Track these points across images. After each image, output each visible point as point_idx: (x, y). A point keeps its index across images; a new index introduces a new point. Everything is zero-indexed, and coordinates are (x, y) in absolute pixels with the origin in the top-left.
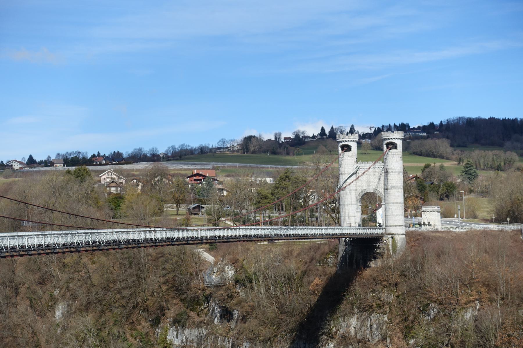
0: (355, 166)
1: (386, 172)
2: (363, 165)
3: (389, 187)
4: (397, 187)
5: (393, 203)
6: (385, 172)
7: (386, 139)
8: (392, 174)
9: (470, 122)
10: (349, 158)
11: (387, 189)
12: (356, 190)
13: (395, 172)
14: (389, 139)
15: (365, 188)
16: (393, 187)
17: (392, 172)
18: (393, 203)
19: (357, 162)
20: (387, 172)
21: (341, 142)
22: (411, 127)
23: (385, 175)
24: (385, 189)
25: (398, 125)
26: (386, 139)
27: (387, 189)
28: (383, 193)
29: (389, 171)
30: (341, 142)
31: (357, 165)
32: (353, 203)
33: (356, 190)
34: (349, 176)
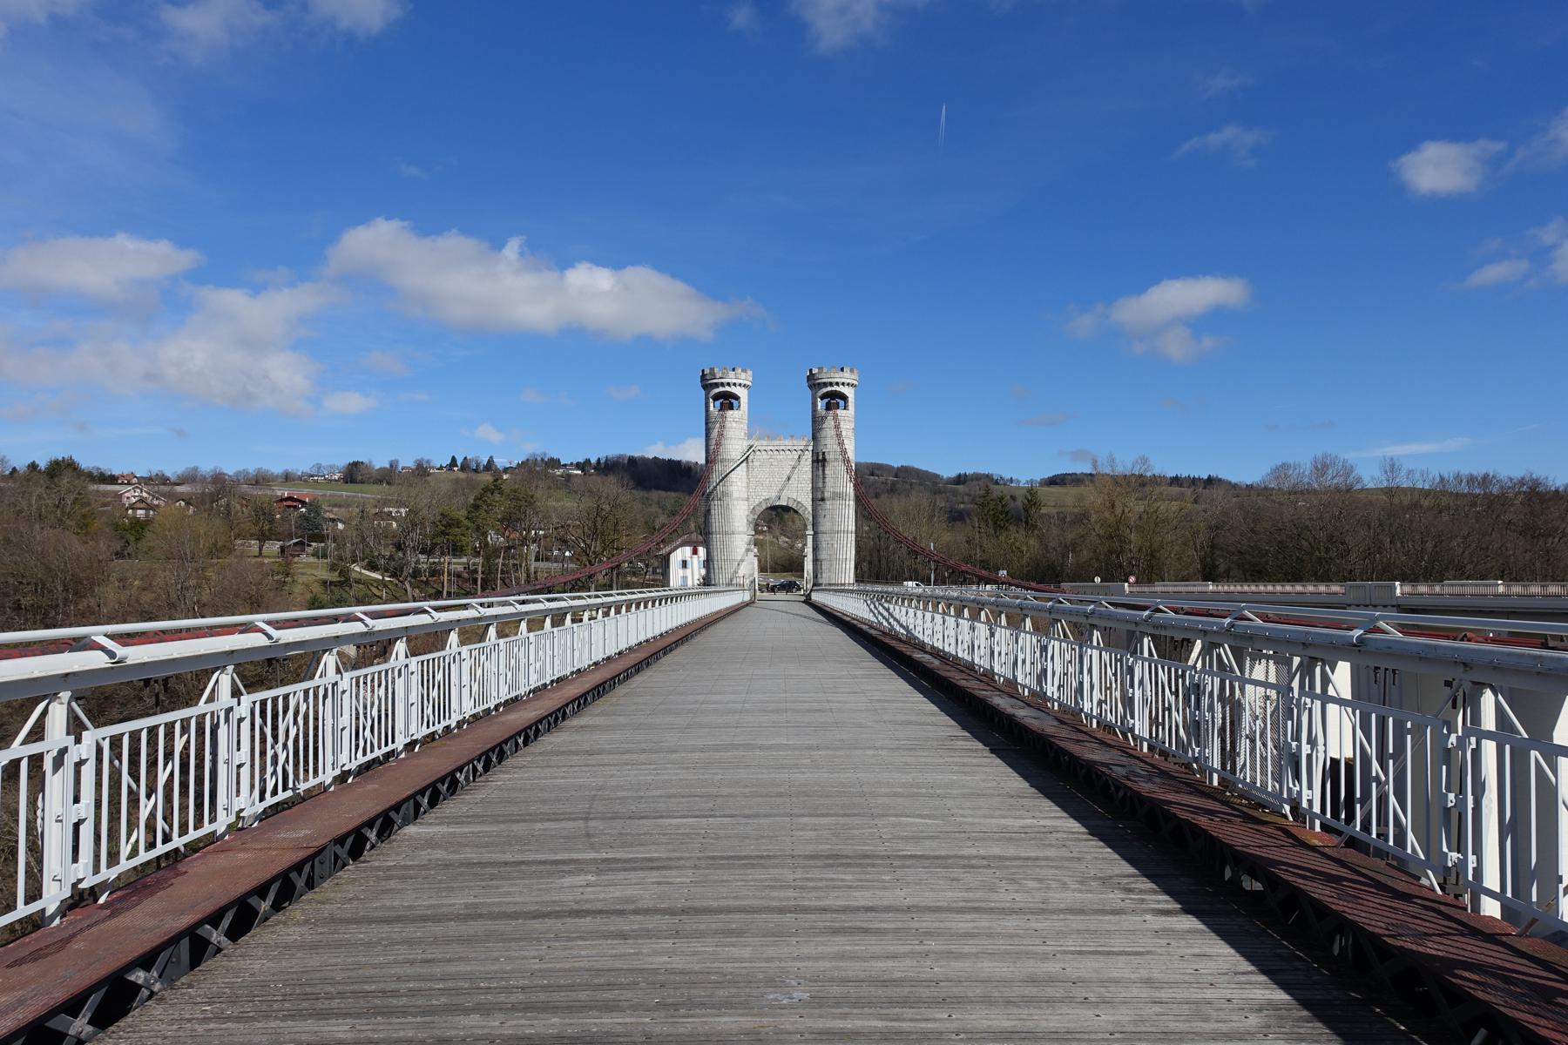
0: (746, 444)
7: (825, 385)
11: (823, 499)
14: (831, 384)
15: (765, 495)
16: (838, 496)
20: (824, 460)
21: (716, 385)
26: (825, 385)
27: (823, 499)
30: (716, 385)
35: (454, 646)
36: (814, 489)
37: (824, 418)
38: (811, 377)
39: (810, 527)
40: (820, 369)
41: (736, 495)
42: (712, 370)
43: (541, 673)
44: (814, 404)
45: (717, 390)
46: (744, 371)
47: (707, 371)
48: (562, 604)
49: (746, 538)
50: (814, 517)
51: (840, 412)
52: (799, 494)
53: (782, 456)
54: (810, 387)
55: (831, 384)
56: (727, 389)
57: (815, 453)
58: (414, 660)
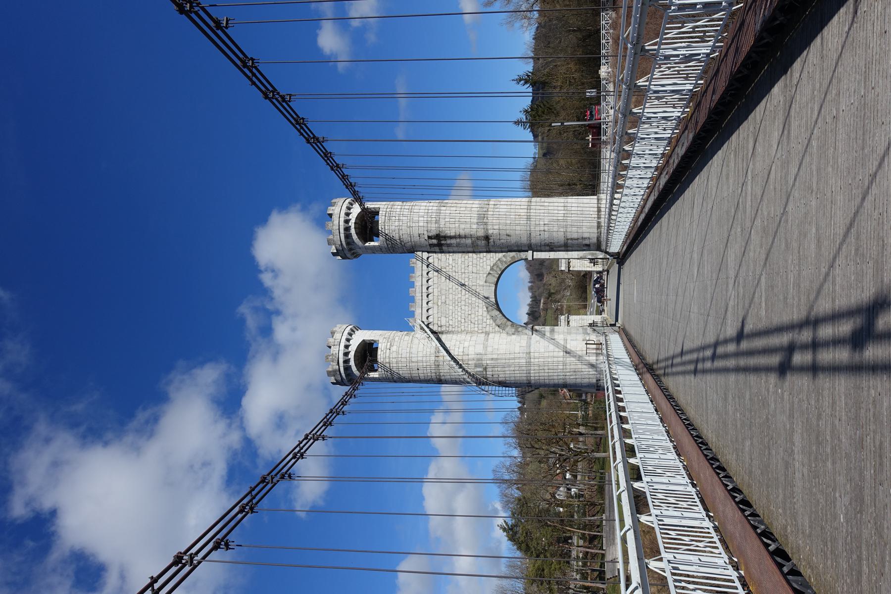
0: (419, 334)
1: (440, 243)
3: (481, 233)
5: (529, 218)
7: (348, 236)
8: (442, 222)
10: (394, 348)
11: (487, 238)
13: (439, 213)
14: (347, 229)
16: (482, 218)
17: (437, 222)
18: (529, 218)
19: (411, 329)
20: (438, 237)
24: (489, 252)
26: (348, 236)
28: (500, 255)
29: (433, 229)
31: (417, 328)
32: (524, 343)
33: (487, 333)
34: (441, 348)
35: (649, 518)
37: (388, 239)
41: (480, 349)
42: (329, 374)
43: (675, 470)
44: (373, 250)
47: (333, 379)
48: (618, 445)
53: (433, 290)
55: (347, 229)
58: (664, 555)
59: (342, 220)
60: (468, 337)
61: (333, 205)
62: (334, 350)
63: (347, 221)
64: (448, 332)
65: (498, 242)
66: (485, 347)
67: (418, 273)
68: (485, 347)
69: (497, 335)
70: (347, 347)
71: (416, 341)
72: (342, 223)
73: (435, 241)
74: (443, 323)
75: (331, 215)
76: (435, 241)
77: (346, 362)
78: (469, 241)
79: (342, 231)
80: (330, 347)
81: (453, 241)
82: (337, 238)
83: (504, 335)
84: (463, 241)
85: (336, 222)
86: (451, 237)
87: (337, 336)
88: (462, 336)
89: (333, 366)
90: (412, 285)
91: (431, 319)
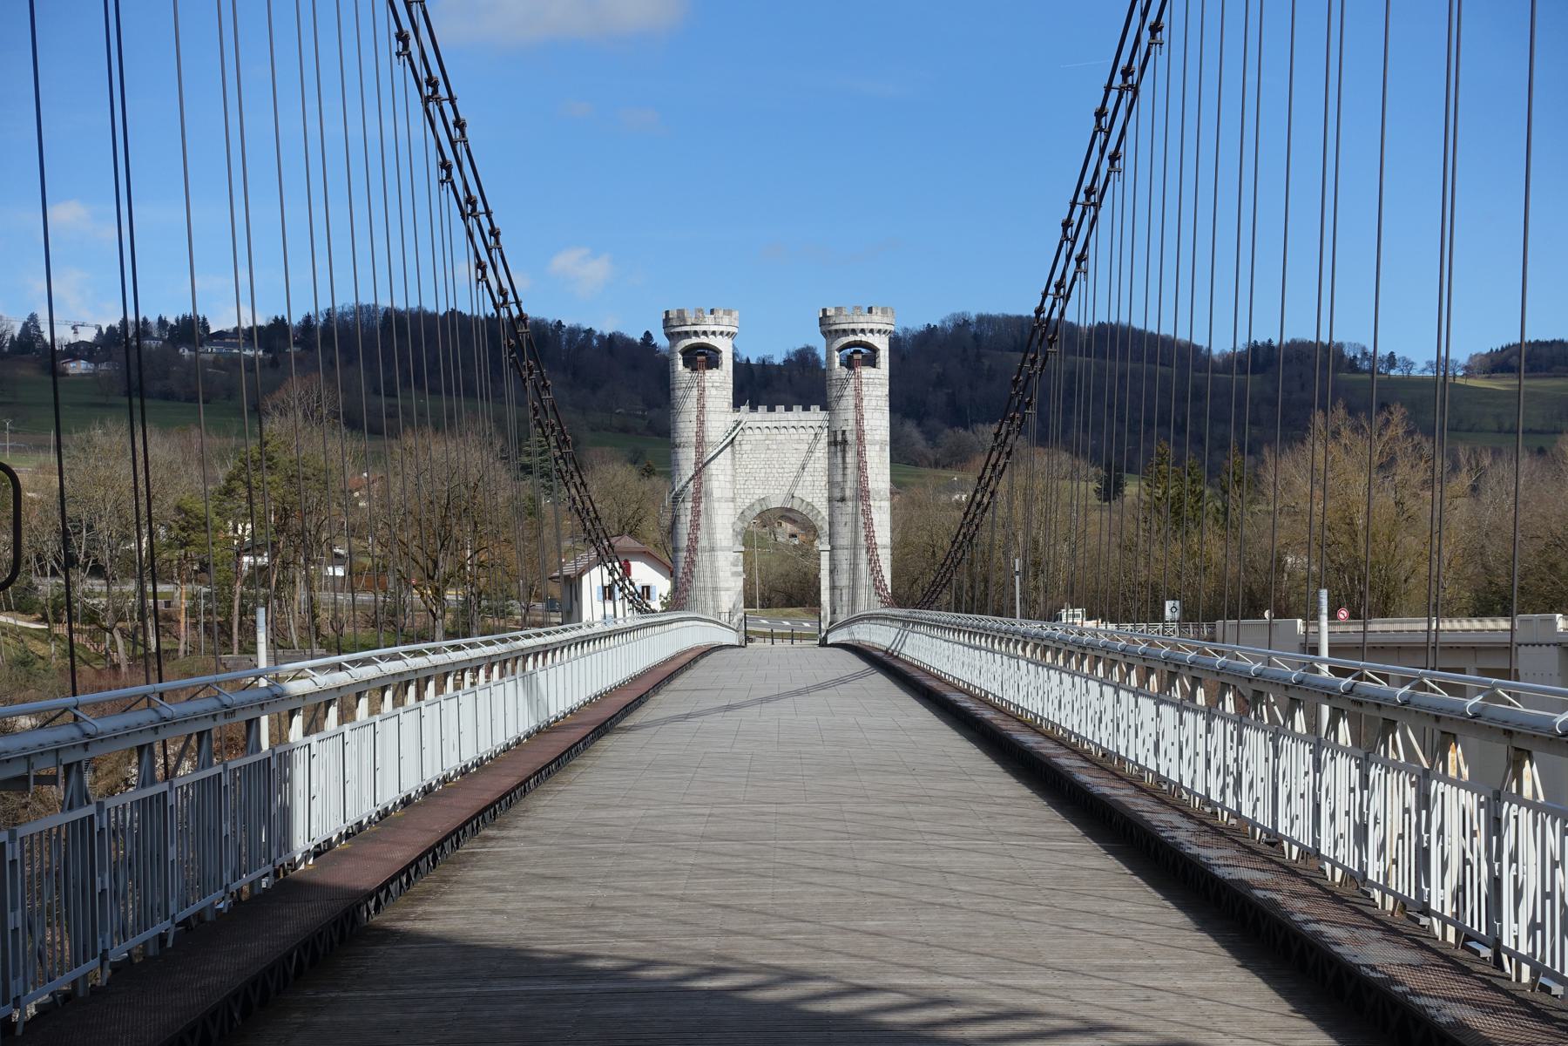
2: (756, 416)
4: (878, 493)
6: (833, 443)
9: (395, 322)
10: (714, 392)
11: (843, 500)
12: (733, 500)
14: (854, 331)
15: (759, 493)
19: (737, 404)
20: (845, 442)
21: (687, 334)
22: (212, 331)
23: (831, 456)
24: (830, 500)
25: (171, 320)
28: (825, 513)
30: (687, 334)
31: (737, 416)
32: (725, 543)
33: (733, 500)
36: (831, 484)
38: (824, 320)
39: (825, 539)
40: (838, 309)
41: (716, 493)
42: (681, 312)
45: (687, 342)
46: (728, 312)
49: (731, 556)
50: (831, 524)
51: (866, 372)
52: (813, 494)
53: (782, 436)
54: (824, 333)
56: (703, 339)
57: (832, 433)
59: (865, 326)
60: (729, 478)
61: (884, 311)
62: (709, 318)
63: (863, 331)
64: (733, 453)
65: (837, 511)
66: (719, 500)
67: (804, 415)
68: (719, 500)
69: (731, 512)
70: (714, 333)
71: (722, 417)
72: (861, 326)
73: (839, 438)
74: (746, 447)
75: (870, 310)
76: (839, 438)
77: (696, 333)
78: (839, 478)
79: (852, 326)
80: (712, 312)
81: (840, 460)
82: (842, 319)
83: (733, 520)
84: (840, 472)
85: (861, 319)
86: (844, 458)
87: (726, 320)
88: (729, 472)
89: (690, 319)
90: (788, 409)
91: (748, 432)
